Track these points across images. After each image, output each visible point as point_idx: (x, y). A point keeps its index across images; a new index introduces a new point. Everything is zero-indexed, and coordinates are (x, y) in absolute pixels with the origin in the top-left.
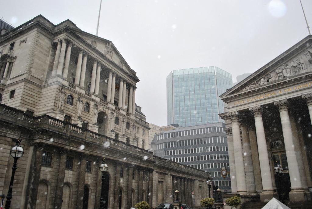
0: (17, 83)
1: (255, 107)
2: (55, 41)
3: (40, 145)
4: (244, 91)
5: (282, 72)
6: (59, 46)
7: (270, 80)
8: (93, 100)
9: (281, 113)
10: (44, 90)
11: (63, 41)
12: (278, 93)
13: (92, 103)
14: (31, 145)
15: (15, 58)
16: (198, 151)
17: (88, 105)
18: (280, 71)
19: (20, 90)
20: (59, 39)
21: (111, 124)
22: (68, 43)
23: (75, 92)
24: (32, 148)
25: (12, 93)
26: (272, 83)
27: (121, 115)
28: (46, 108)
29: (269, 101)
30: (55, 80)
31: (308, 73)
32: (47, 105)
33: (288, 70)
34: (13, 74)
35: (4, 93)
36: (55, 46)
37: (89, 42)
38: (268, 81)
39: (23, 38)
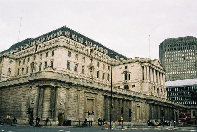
0: (135, 82)
3: (151, 103)
8: (155, 85)
10: (142, 84)
13: (155, 86)
14: (148, 103)
15: (130, 72)
17: (154, 87)
19: (137, 85)
21: (160, 92)
22: (148, 66)
23: (152, 84)
24: (148, 105)
25: (134, 86)
27: (162, 87)
30: (147, 81)
36: (143, 67)
37: (152, 63)
39: (132, 65)
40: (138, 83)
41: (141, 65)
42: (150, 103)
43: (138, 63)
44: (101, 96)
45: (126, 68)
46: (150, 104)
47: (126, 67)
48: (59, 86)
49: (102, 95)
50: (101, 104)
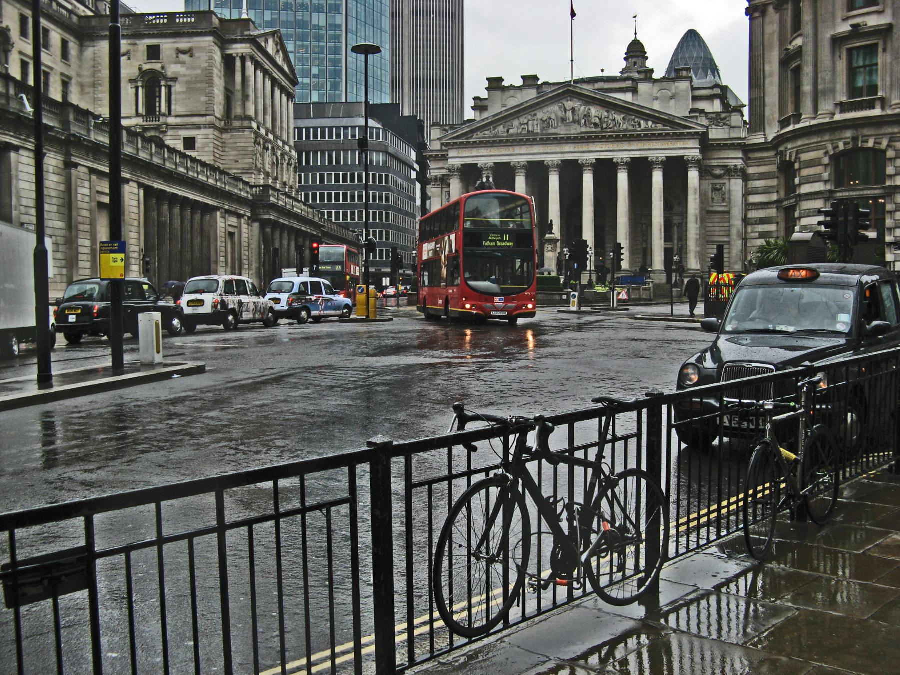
0: (198, 127)
1: (486, 164)
2: (229, 52)
4: (475, 138)
5: (527, 124)
6: (238, 64)
7: (511, 131)
9: (517, 178)
11: (248, 59)
12: (518, 150)
16: (314, 177)
18: (526, 122)
20: (240, 51)
24: (256, 225)
26: (512, 135)
28: (240, 166)
29: (505, 160)
31: (557, 134)
32: (240, 161)
33: (536, 122)
34: (177, 108)
35: (168, 138)
38: (508, 131)
40: (210, 131)
41: (222, 49)
42: (266, 217)
43: (211, 39)
44: (136, 191)
45: (149, 58)
46: (264, 224)
47: (154, 53)
48: (15, 142)
49: (140, 185)
50: (136, 223)
